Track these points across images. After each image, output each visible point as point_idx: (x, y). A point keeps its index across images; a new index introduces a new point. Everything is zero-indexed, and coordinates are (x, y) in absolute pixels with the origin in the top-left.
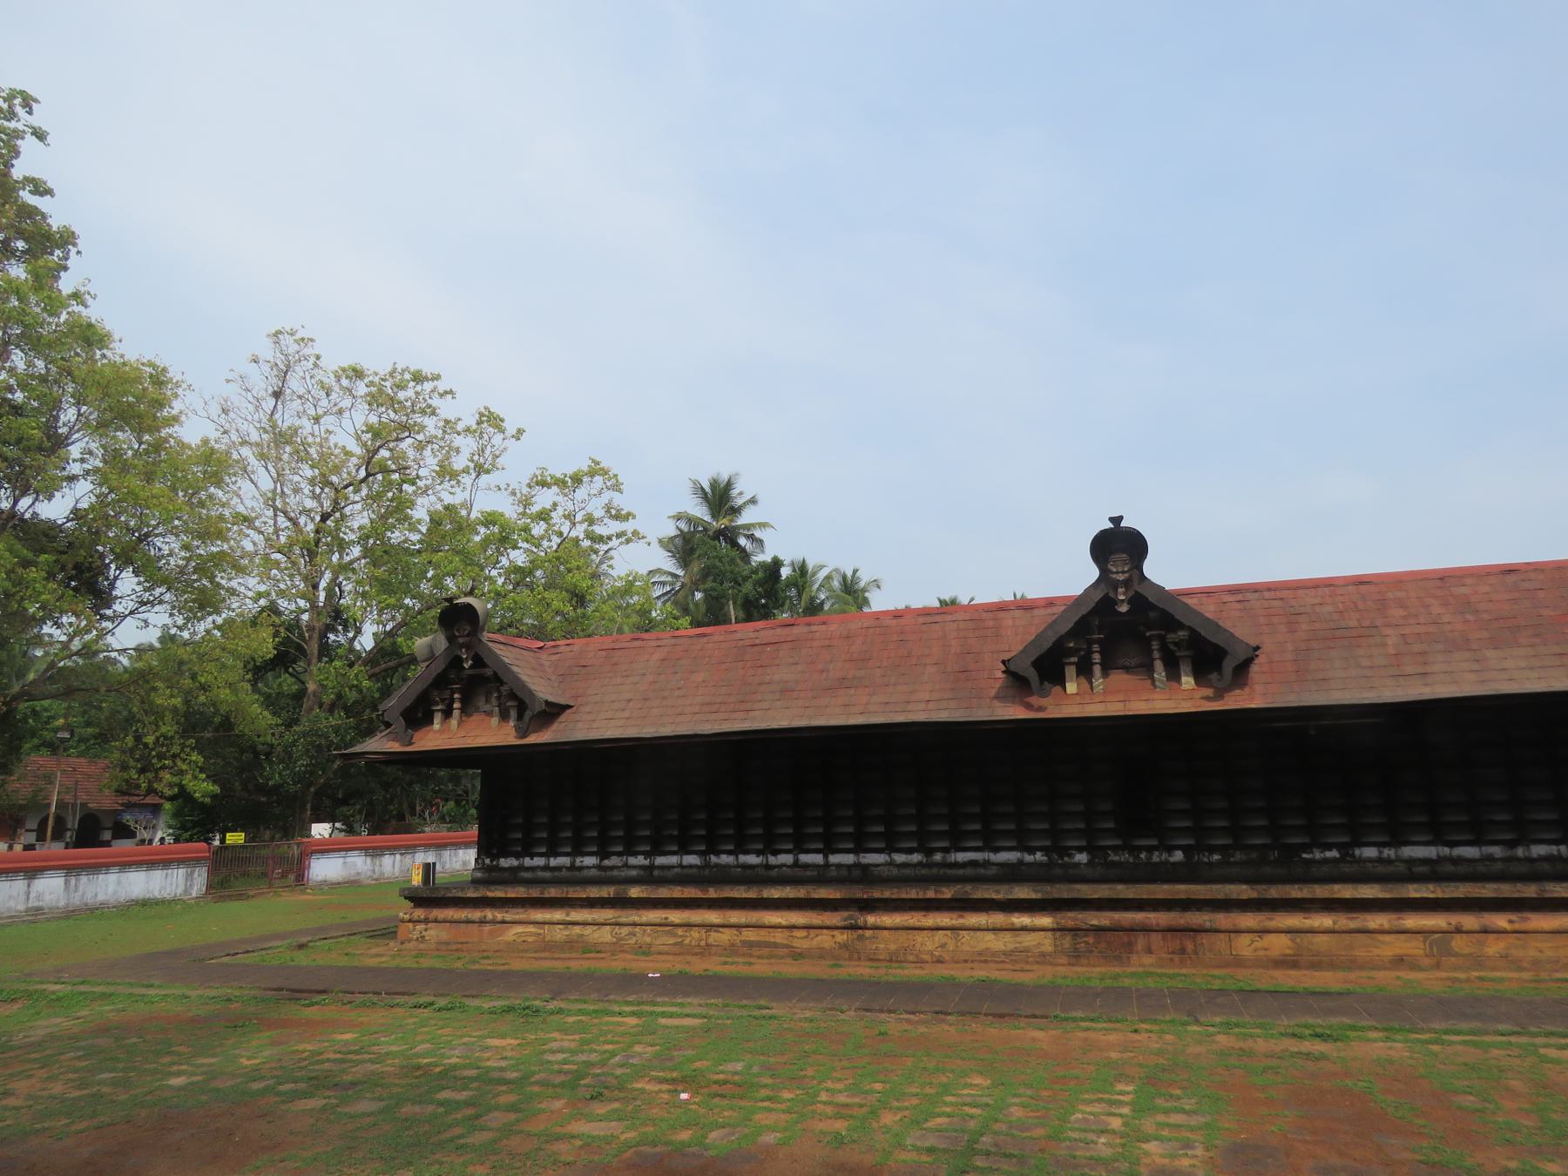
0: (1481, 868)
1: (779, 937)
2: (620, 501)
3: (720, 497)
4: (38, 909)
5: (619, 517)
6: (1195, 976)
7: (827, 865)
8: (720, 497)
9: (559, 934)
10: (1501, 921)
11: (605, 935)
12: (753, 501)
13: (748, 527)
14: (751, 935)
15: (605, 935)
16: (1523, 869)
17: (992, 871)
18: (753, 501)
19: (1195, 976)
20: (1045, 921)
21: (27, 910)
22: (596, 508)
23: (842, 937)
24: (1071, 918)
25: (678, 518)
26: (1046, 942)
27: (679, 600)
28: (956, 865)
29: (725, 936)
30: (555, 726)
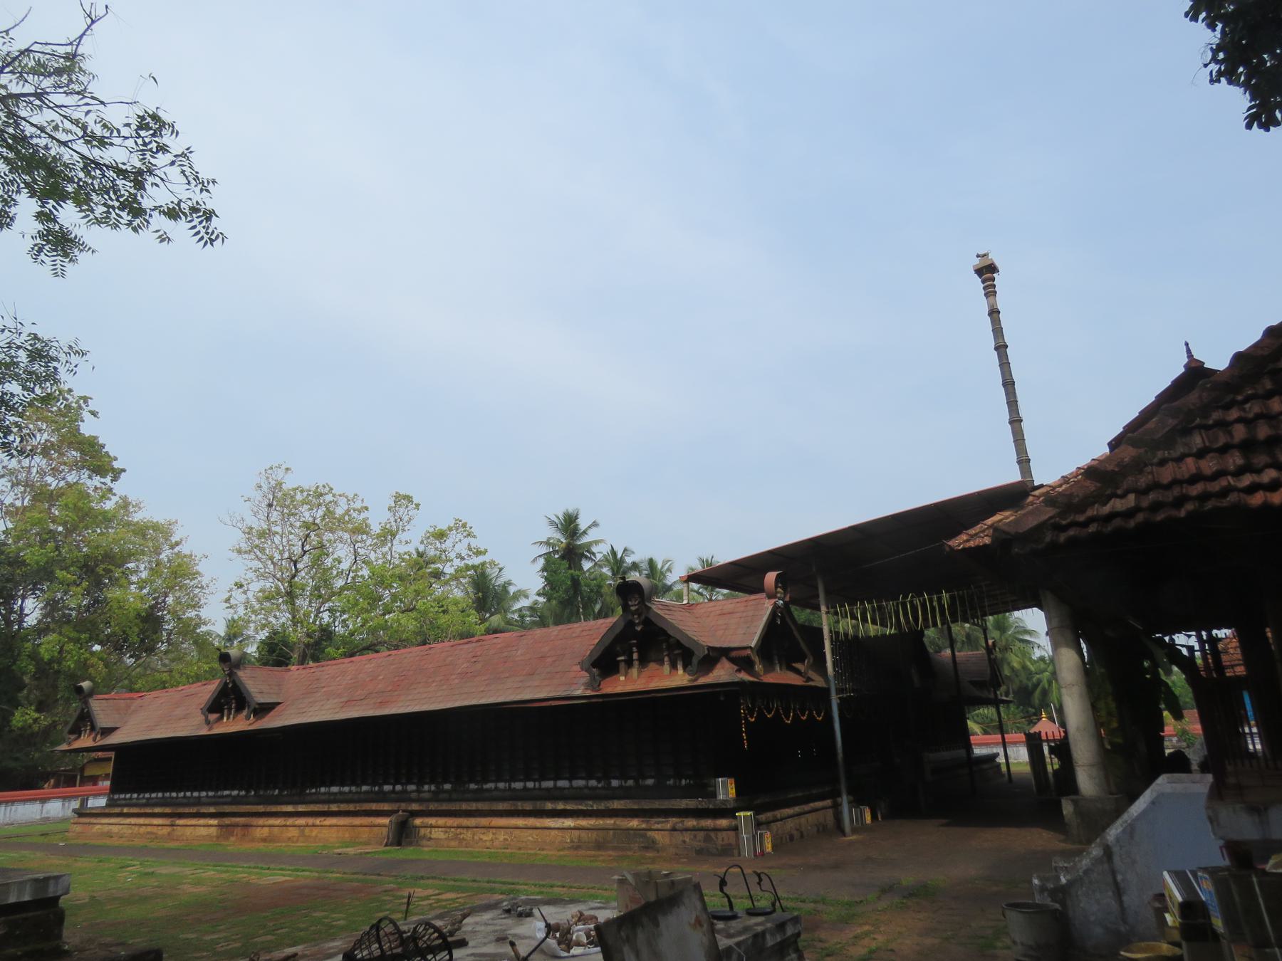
0: (339, 797)
1: (154, 829)
2: (474, 543)
3: (569, 525)
4: (48, 819)
5: (478, 553)
6: (246, 847)
7: (571, 787)
8: (569, 525)
9: (106, 828)
10: (318, 821)
11: (115, 829)
12: (595, 524)
13: (590, 544)
14: (149, 829)
15: (115, 829)
16: (356, 797)
17: (229, 800)
18: (595, 524)
19: (246, 847)
20: (214, 822)
21: (42, 819)
22: (462, 548)
23: (169, 829)
24: (227, 821)
25: (548, 543)
26: (213, 831)
27: (259, 660)
28: (222, 797)
29: (143, 830)
30: (266, 719)
